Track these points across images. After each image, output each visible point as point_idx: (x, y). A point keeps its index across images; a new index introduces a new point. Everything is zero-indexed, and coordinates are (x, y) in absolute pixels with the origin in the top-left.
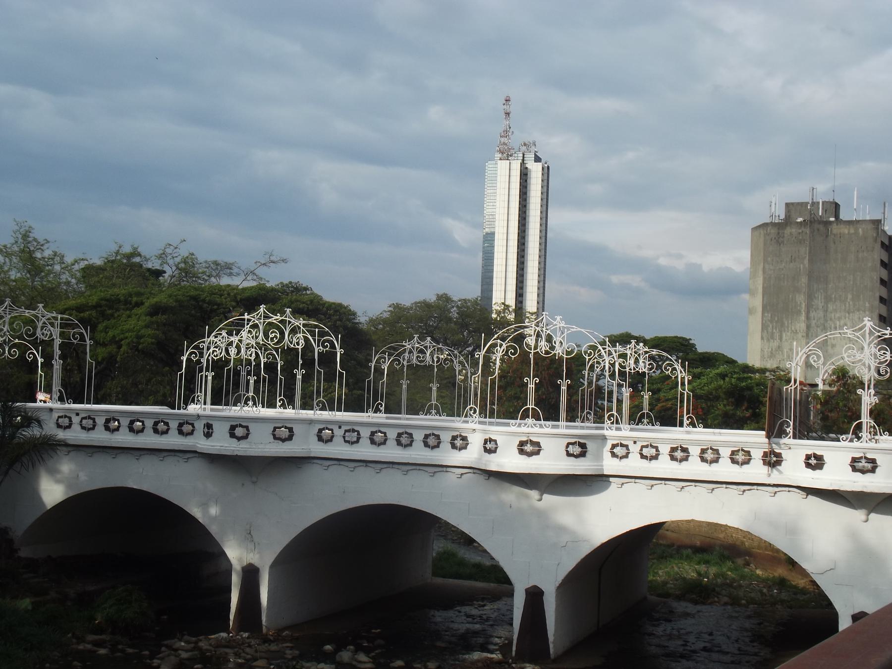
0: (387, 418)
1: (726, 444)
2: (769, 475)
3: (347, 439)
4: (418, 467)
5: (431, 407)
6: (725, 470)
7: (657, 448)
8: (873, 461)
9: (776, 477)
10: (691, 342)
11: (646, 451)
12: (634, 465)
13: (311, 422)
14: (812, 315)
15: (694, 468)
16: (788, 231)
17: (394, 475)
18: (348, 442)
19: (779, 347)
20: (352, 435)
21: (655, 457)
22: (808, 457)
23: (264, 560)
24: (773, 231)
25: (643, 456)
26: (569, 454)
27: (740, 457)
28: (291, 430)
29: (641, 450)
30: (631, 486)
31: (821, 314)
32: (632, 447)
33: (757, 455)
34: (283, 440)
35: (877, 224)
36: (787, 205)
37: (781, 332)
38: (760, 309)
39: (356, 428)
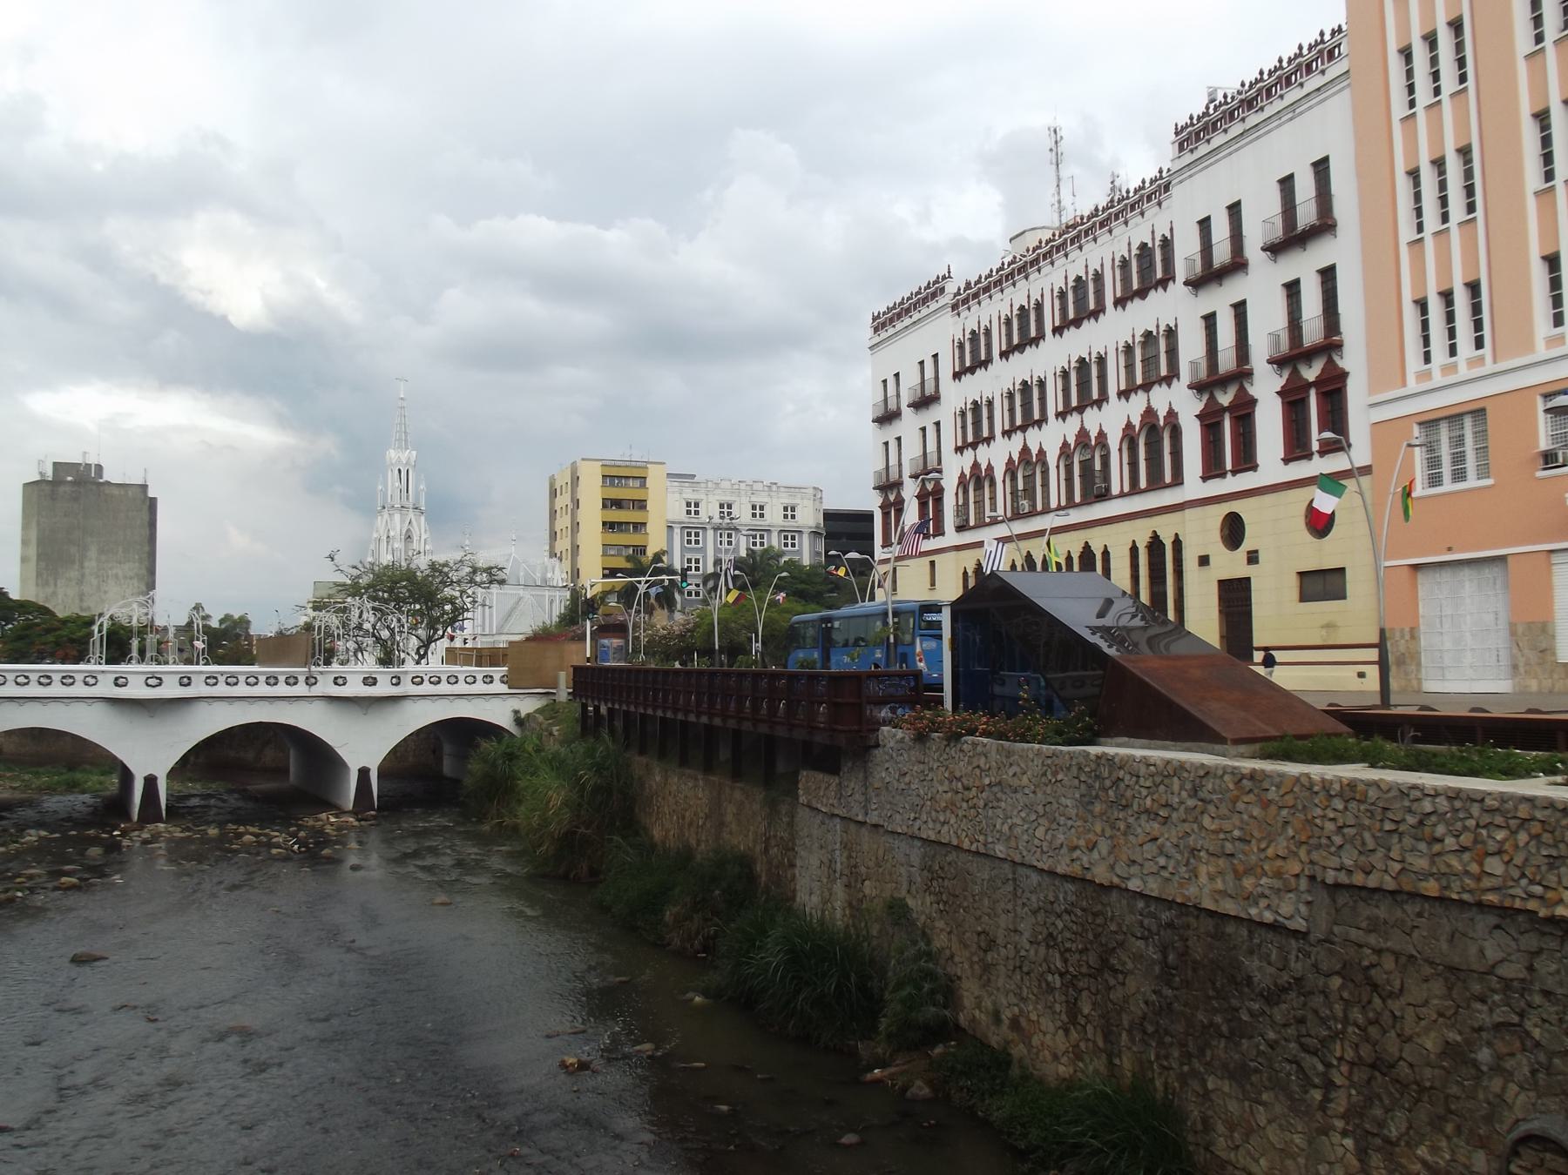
1: (282, 673)
5: (131, 658)
6: (282, 689)
7: (256, 678)
8: (375, 679)
9: (317, 690)
14: (86, 564)
15: (262, 689)
16: (62, 489)
21: (236, 684)
22: (336, 678)
24: (47, 488)
25: (228, 684)
26: (181, 685)
27: (292, 681)
30: (217, 705)
31: (94, 564)
33: (302, 679)
35: (144, 487)
36: (55, 464)
37: (56, 580)
38: (34, 558)
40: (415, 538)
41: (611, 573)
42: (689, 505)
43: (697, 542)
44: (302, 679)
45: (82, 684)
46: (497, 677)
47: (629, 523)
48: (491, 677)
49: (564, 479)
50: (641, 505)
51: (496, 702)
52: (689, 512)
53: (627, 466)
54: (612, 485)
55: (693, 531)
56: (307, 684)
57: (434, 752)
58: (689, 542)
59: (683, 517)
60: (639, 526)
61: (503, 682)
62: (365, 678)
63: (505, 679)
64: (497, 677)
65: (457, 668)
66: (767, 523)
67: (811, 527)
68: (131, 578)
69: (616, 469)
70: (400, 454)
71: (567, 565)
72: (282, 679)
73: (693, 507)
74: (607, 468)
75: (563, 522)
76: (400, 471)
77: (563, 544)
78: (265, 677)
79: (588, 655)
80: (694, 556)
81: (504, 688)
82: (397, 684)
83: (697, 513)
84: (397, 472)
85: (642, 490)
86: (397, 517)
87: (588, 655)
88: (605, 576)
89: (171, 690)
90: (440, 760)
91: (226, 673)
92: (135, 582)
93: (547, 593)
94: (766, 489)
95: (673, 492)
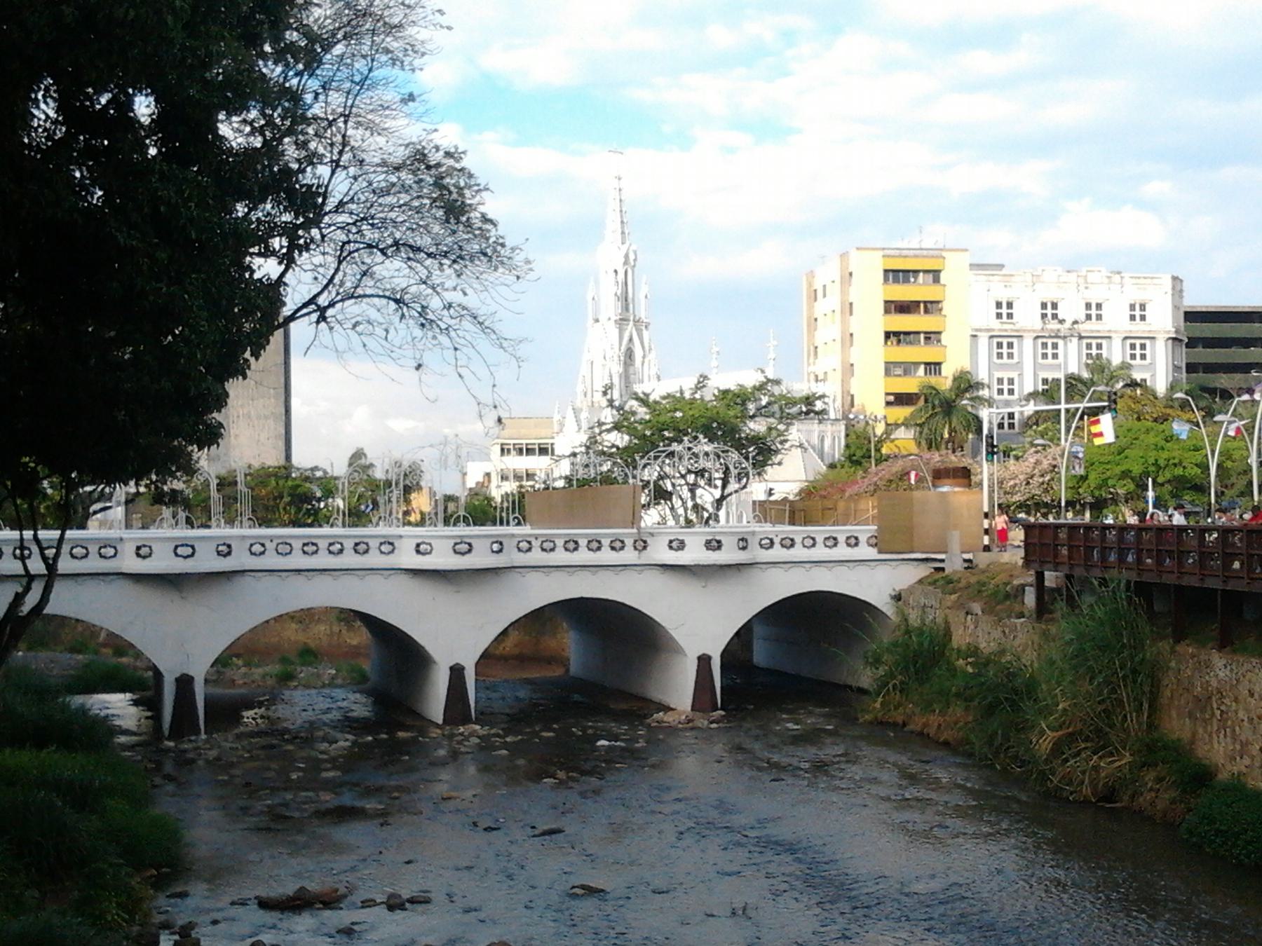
2: (639, 558)
8: (719, 542)
11: (545, 545)
12: (536, 557)
13: (244, 538)
17: (326, 579)
18: (281, 554)
21: (552, 550)
23: (199, 670)
25: (543, 550)
28: (229, 546)
32: (534, 543)
33: (629, 542)
34: (225, 556)
39: (288, 541)
42: (999, 305)
43: (1010, 356)
44: (629, 542)
45: (353, 551)
46: (863, 538)
47: (918, 333)
48: (835, 539)
51: (862, 570)
52: (999, 316)
53: (916, 256)
54: (896, 281)
56: (635, 548)
58: (1045, 356)
59: (1038, 324)
63: (873, 541)
66: (1107, 328)
67: (1169, 332)
68: (266, 418)
69: (901, 260)
72: (583, 542)
73: (1004, 309)
74: (891, 260)
78: (586, 542)
79: (986, 509)
80: (1005, 375)
81: (872, 553)
82: (744, 548)
83: (1010, 316)
85: (936, 288)
87: (986, 509)
88: (888, 404)
92: (271, 422)
94: (1106, 280)
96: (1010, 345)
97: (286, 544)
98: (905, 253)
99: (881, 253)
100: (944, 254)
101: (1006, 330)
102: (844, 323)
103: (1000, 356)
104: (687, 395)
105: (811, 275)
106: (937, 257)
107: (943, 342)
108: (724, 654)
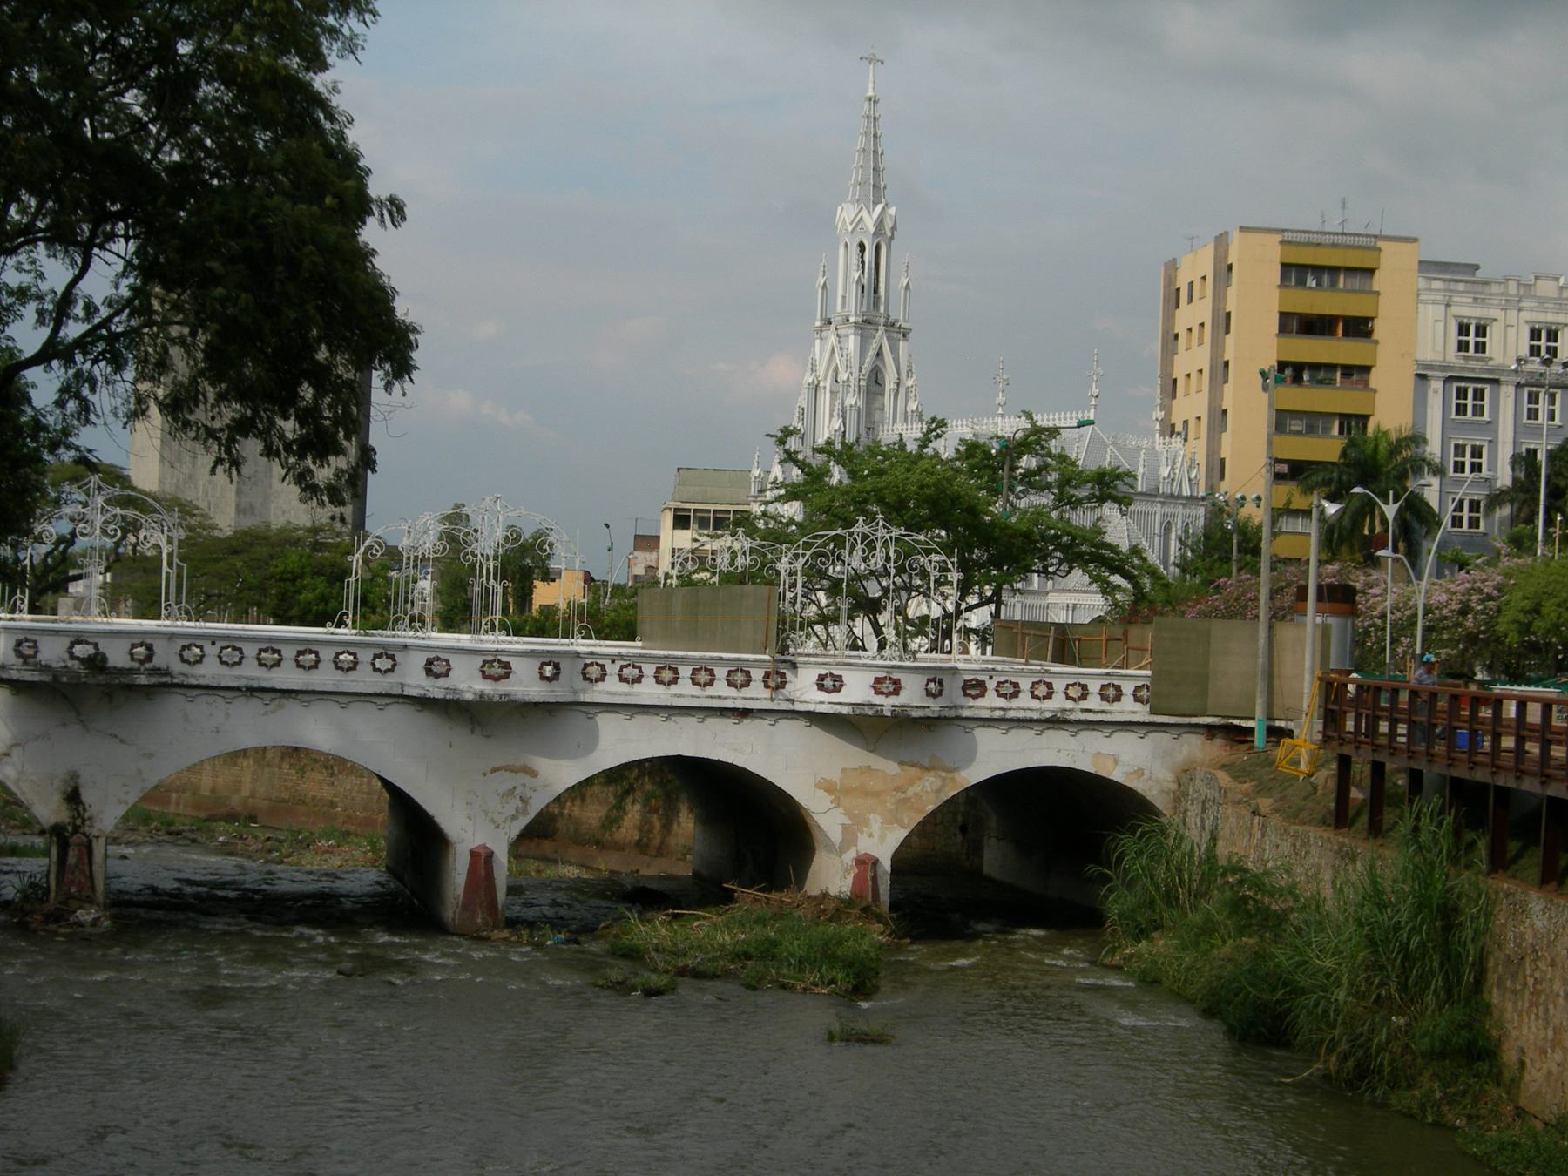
0: (32, 620)
3: (224, 659)
4: (363, 698)
10: (126, 473)
13: (171, 636)
18: (226, 663)
19: (190, 477)
20: (307, 657)
21: (638, 680)
29: (621, 670)
40: (889, 385)
41: (1295, 472)
42: (1463, 329)
43: (1478, 411)
46: (1128, 688)
49: (1197, 266)
50: (1359, 328)
52: (1463, 346)
53: (1334, 245)
54: (1301, 283)
55: (1471, 388)
56: (767, 686)
57: (963, 829)
60: (1357, 373)
61: (1137, 699)
62: (878, 680)
64: (1128, 688)
65: (1018, 664)
70: (864, 213)
71: (1199, 448)
73: (1472, 334)
75: (1193, 359)
76: (862, 247)
77: (1191, 405)
81: (1142, 713)
83: (1480, 347)
84: (855, 250)
86: (852, 343)
88: (1278, 477)
89: (526, 685)
90: (976, 849)
91: (621, 656)
93: (1158, 508)
95: (1434, 302)
96: (1479, 395)
97: (234, 648)
98: (1315, 238)
99: (1279, 238)
100: (1380, 244)
101: (1473, 370)
102: (1217, 347)
103: (1461, 410)
104: (912, 447)
105: (1172, 267)
106: (1368, 248)
107: (1372, 384)
108: (896, 858)
